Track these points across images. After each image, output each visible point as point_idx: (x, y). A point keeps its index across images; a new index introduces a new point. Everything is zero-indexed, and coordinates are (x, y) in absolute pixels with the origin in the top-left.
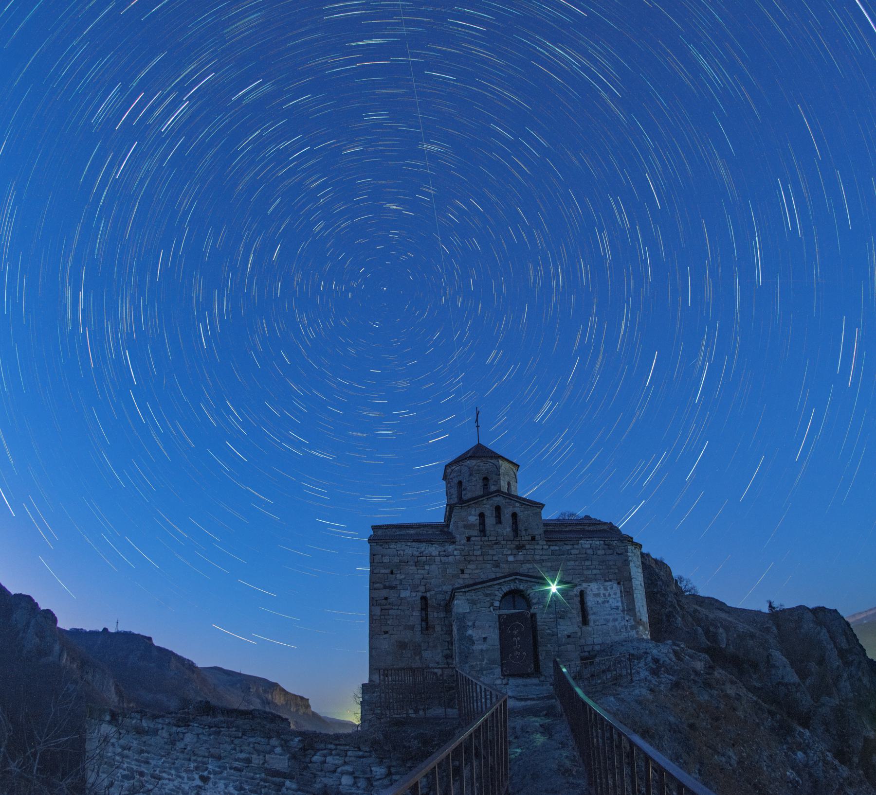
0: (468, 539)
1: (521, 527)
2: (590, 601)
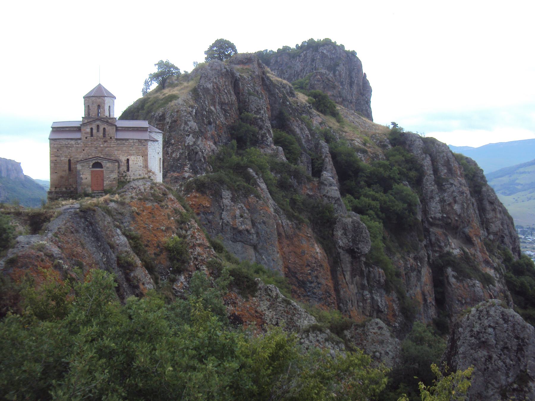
0: (86, 138)
1: (106, 134)
2: (130, 162)
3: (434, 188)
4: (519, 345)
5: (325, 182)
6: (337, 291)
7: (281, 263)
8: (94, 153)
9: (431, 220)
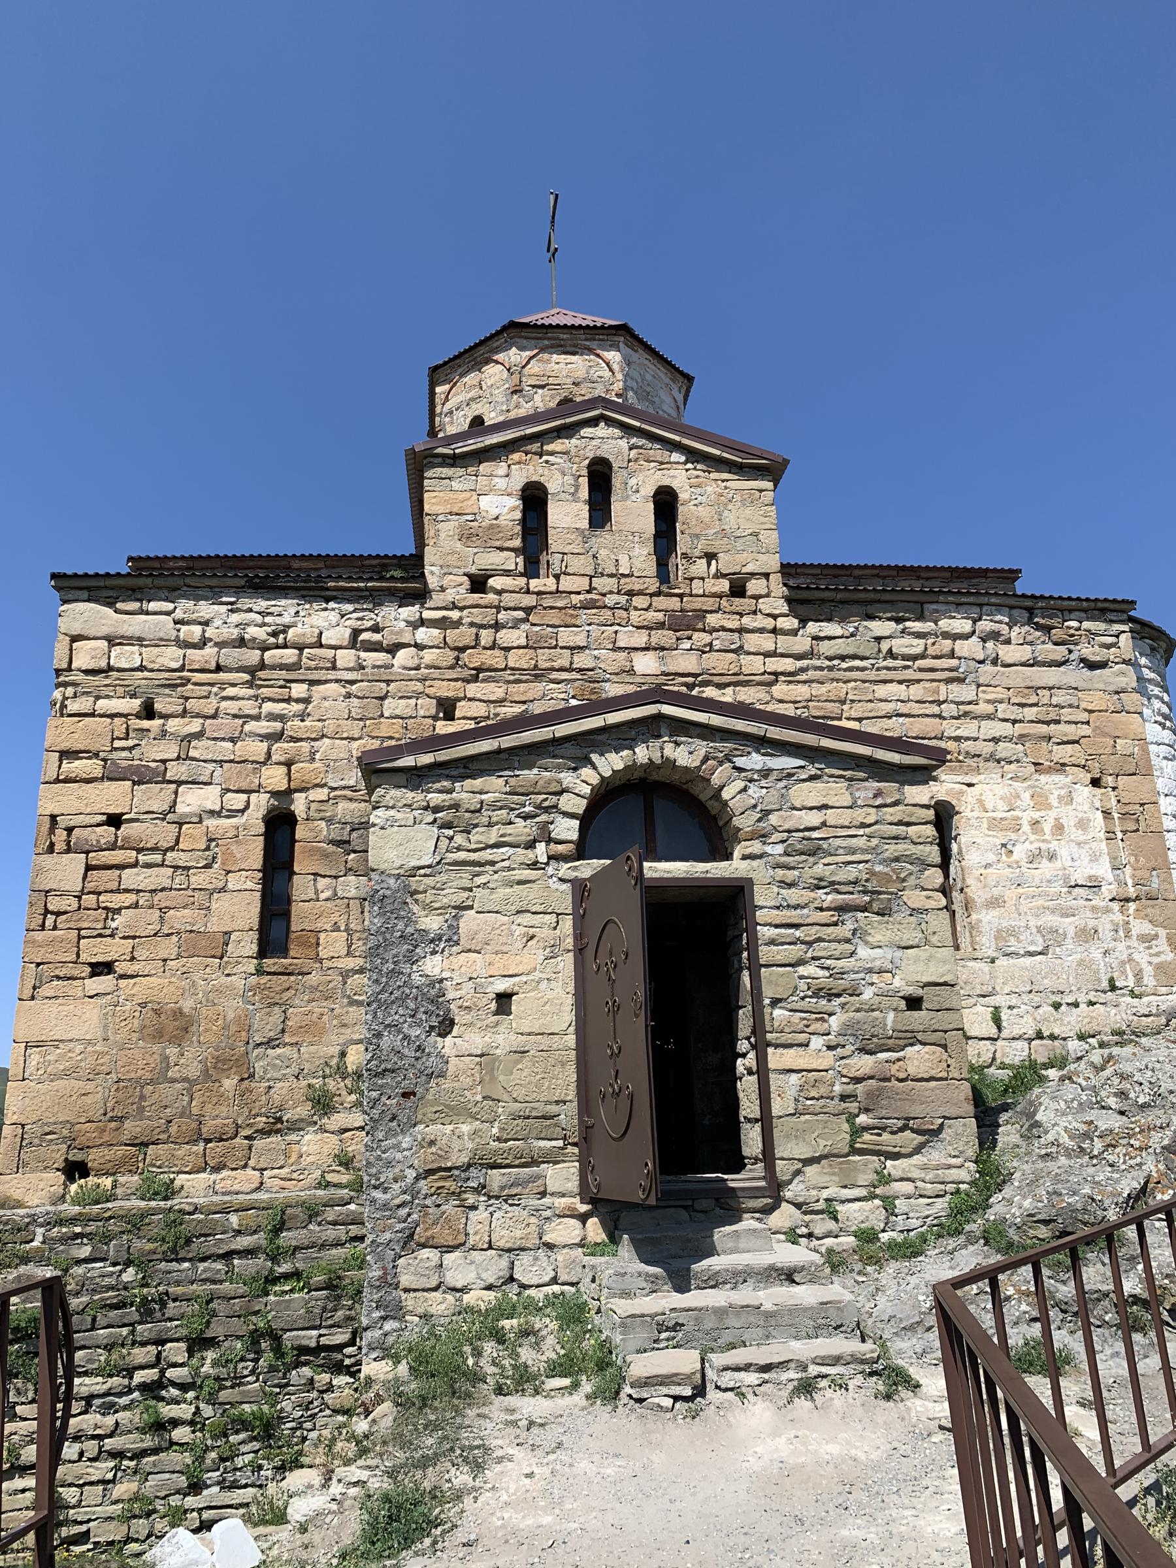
0: (478, 583)
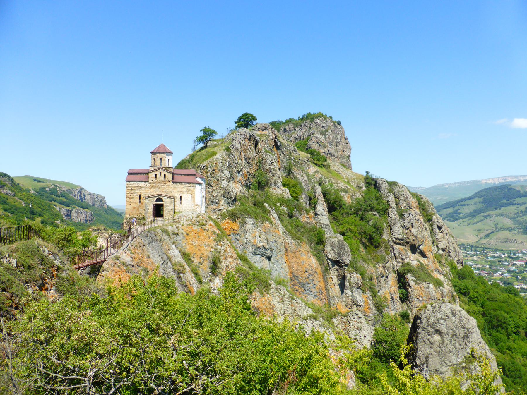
3: (397, 217)
4: (465, 333)
5: (318, 213)
6: (328, 290)
7: (287, 269)
8: (157, 192)
9: (394, 239)
